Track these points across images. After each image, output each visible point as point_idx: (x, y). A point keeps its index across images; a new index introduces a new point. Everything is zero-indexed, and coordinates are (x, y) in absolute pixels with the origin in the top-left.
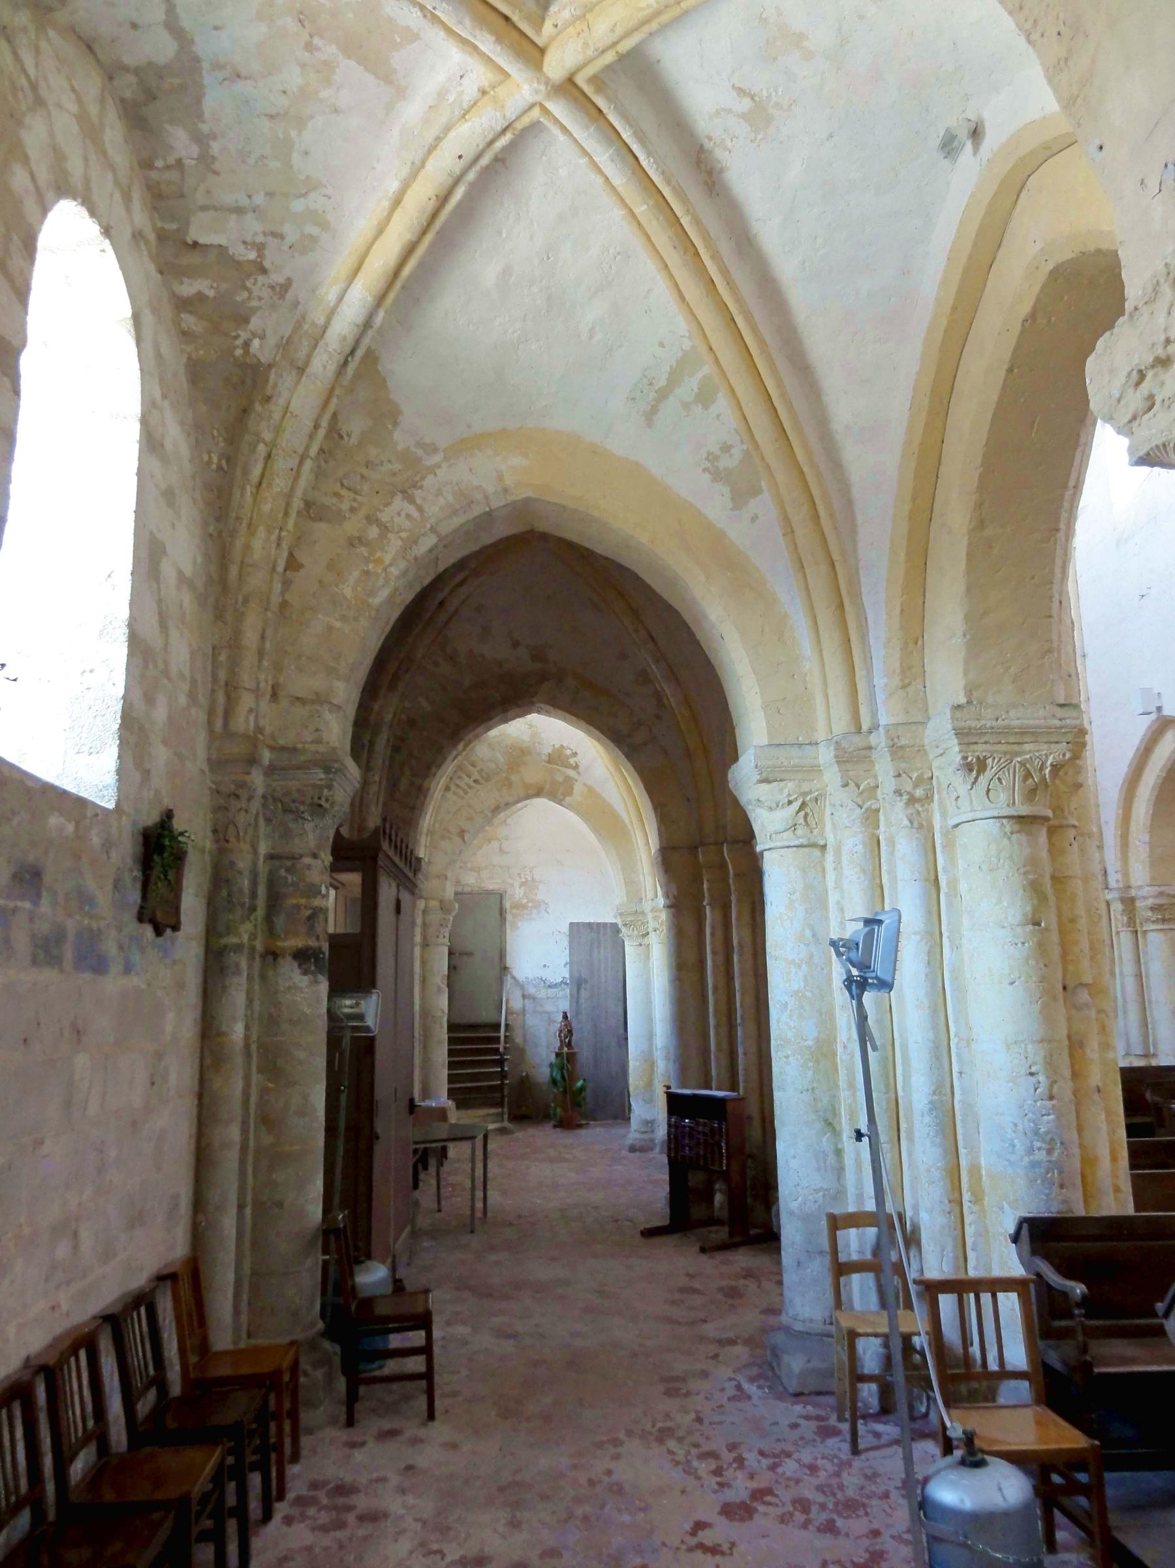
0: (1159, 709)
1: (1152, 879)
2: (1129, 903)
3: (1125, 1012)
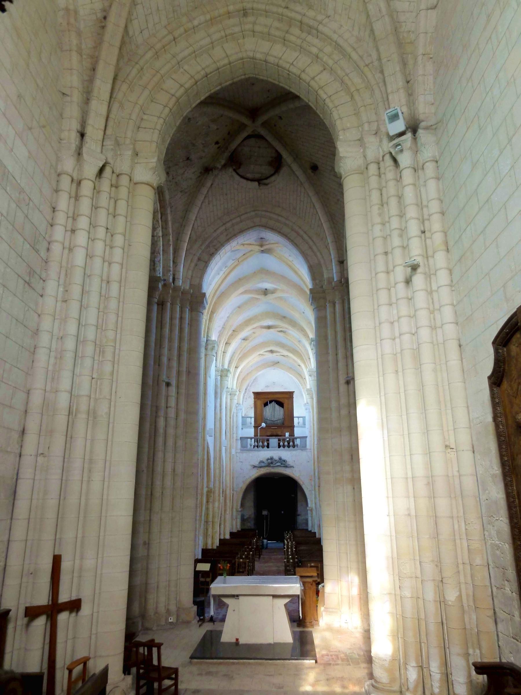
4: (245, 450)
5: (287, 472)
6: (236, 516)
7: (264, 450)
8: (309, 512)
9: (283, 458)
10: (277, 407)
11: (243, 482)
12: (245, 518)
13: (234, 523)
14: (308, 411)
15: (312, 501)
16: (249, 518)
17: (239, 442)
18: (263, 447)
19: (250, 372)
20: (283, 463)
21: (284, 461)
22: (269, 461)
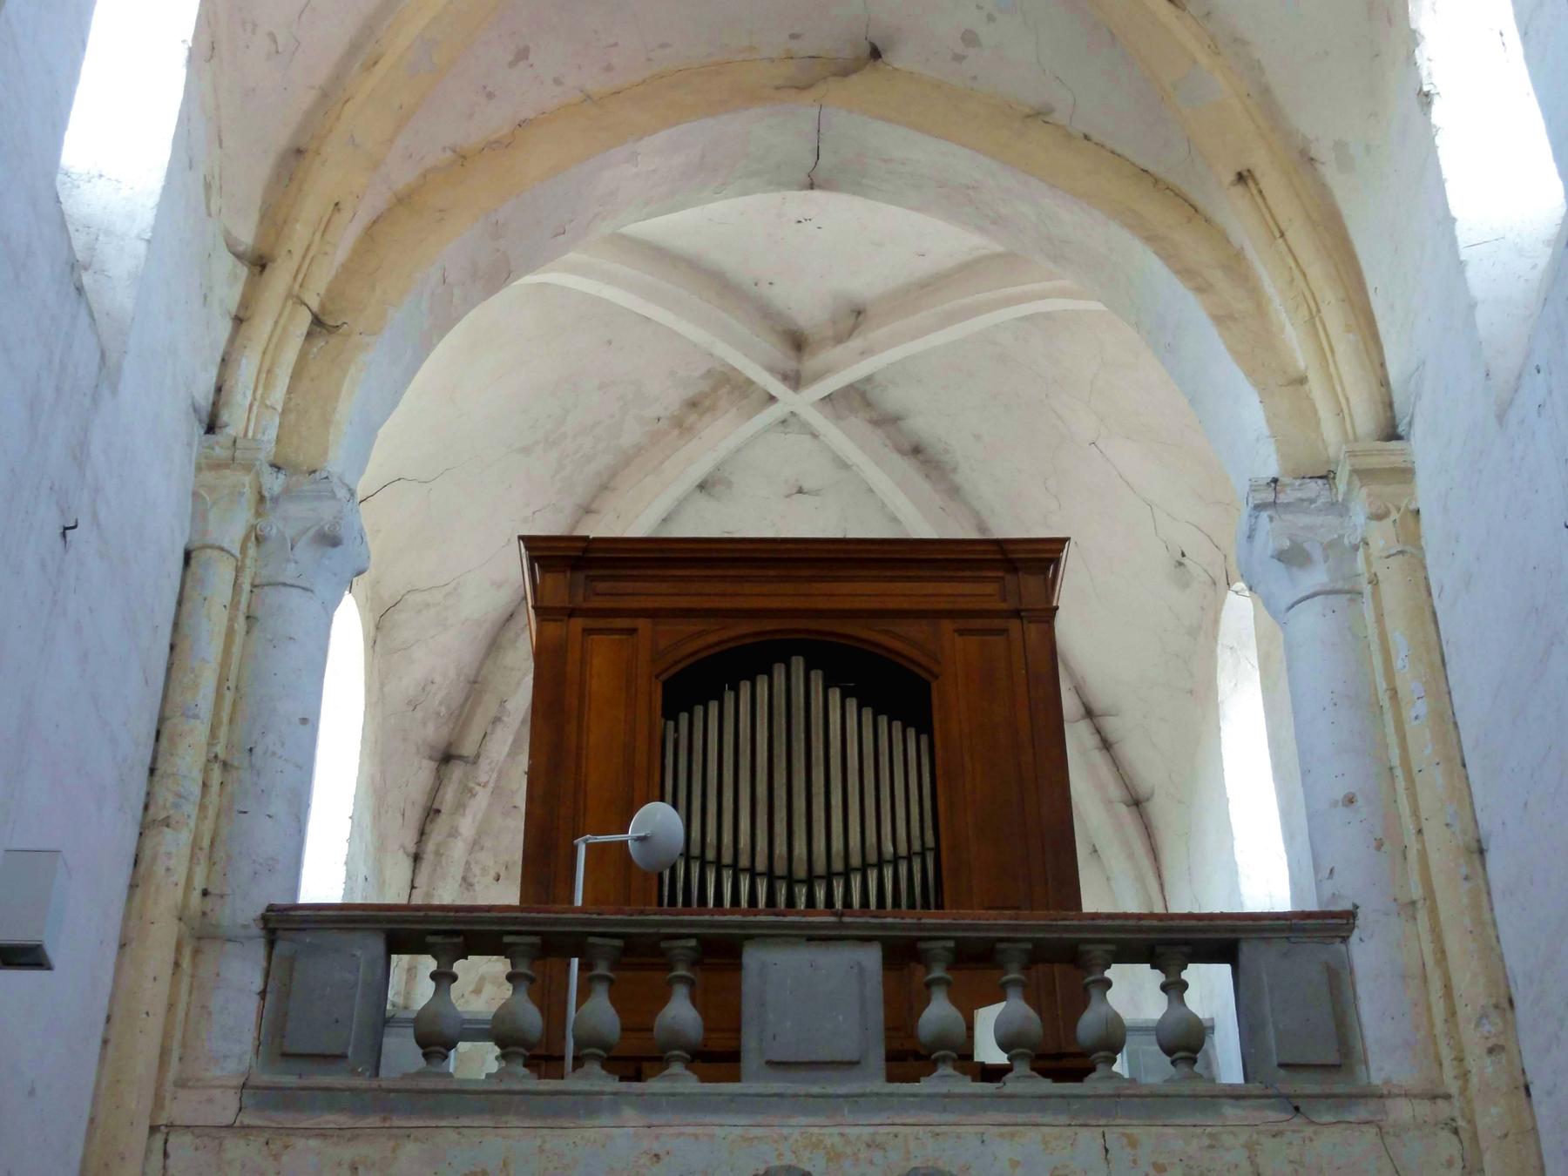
4: (330, 1098)
7: (649, 1104)
10: (843, 719)
14: (1317, 577)
17: (243, 972)
18: (633, 1061)
19: (499, 146)
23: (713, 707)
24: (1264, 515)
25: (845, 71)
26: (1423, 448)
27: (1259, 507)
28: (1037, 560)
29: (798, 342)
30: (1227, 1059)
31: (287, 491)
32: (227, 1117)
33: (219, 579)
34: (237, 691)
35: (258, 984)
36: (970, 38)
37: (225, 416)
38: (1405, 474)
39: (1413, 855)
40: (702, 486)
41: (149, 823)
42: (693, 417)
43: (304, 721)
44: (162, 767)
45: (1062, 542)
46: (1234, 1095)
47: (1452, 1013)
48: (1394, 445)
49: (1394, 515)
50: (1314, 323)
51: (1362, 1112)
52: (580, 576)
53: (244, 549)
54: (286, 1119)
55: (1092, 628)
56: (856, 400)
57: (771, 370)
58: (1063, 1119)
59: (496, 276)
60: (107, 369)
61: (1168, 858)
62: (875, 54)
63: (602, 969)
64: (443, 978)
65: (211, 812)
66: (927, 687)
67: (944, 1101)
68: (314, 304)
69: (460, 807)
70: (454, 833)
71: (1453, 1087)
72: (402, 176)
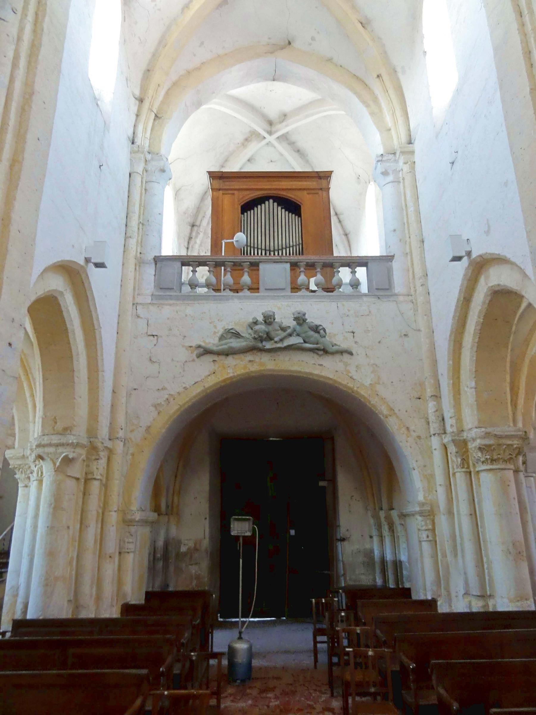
0: (469, 254)
1: (479, 421)
2: (462, 445)
3: (463, 550)
4: (171, 297)
5: (326, 369)
6: (121, 543)
7: (240, 298)
8: (417, 523)
9: (312, 318)
10: (282, 214)
11: (156, 406)
12: (183, 549)
13: (109, 570)
14: (391, 178)
15: (430, 478)
16: (196, 549)
17: (150, 271)
19: (198, 69)
20: (313, 339)
21: (316, 329)
22: (261, 327)
23: (252, 211)
24: (379, 163)
25: (282, 48)
26: (417, 146)
27: (378, 161)
28: (326, 176)
29: (271, 123)
30: (364, 288)
31: (152, 159)
32: (149, 301)
33: (138, 180)
34: (144, 206)
35: (154, 273)
36: (313, 39)
37: (136, 140)
38: (412, 152)
39: (408, 243)
40: (249, 160)
41: (127, 238)
42: (246, 143)
43: (160, 214)
44: (128, 224)
45: (332, 172)
46: (365, 295)
47: (414, 277)
48: (410, 145)
49: (409, 163)
50: (393, 114)
51: (392, 299)
52: (221, 181)
53: (143, 173)
54: (161, 302)
55: (339, 194)
56: (284, 138)
57: (264, 130)
58: (329, 300)
59: (198, 104)
60: (106, 125)
61: (352, 246)
62: (290, 43)
63: (229, 269)
64: (194, 271)
65: (140, 235)
66: (300, 206)
67: (303, 297)
68: (155, 111)
69: (196, 237)
70: (195, 243)
71: (412, 293)
72: (174, 77)
